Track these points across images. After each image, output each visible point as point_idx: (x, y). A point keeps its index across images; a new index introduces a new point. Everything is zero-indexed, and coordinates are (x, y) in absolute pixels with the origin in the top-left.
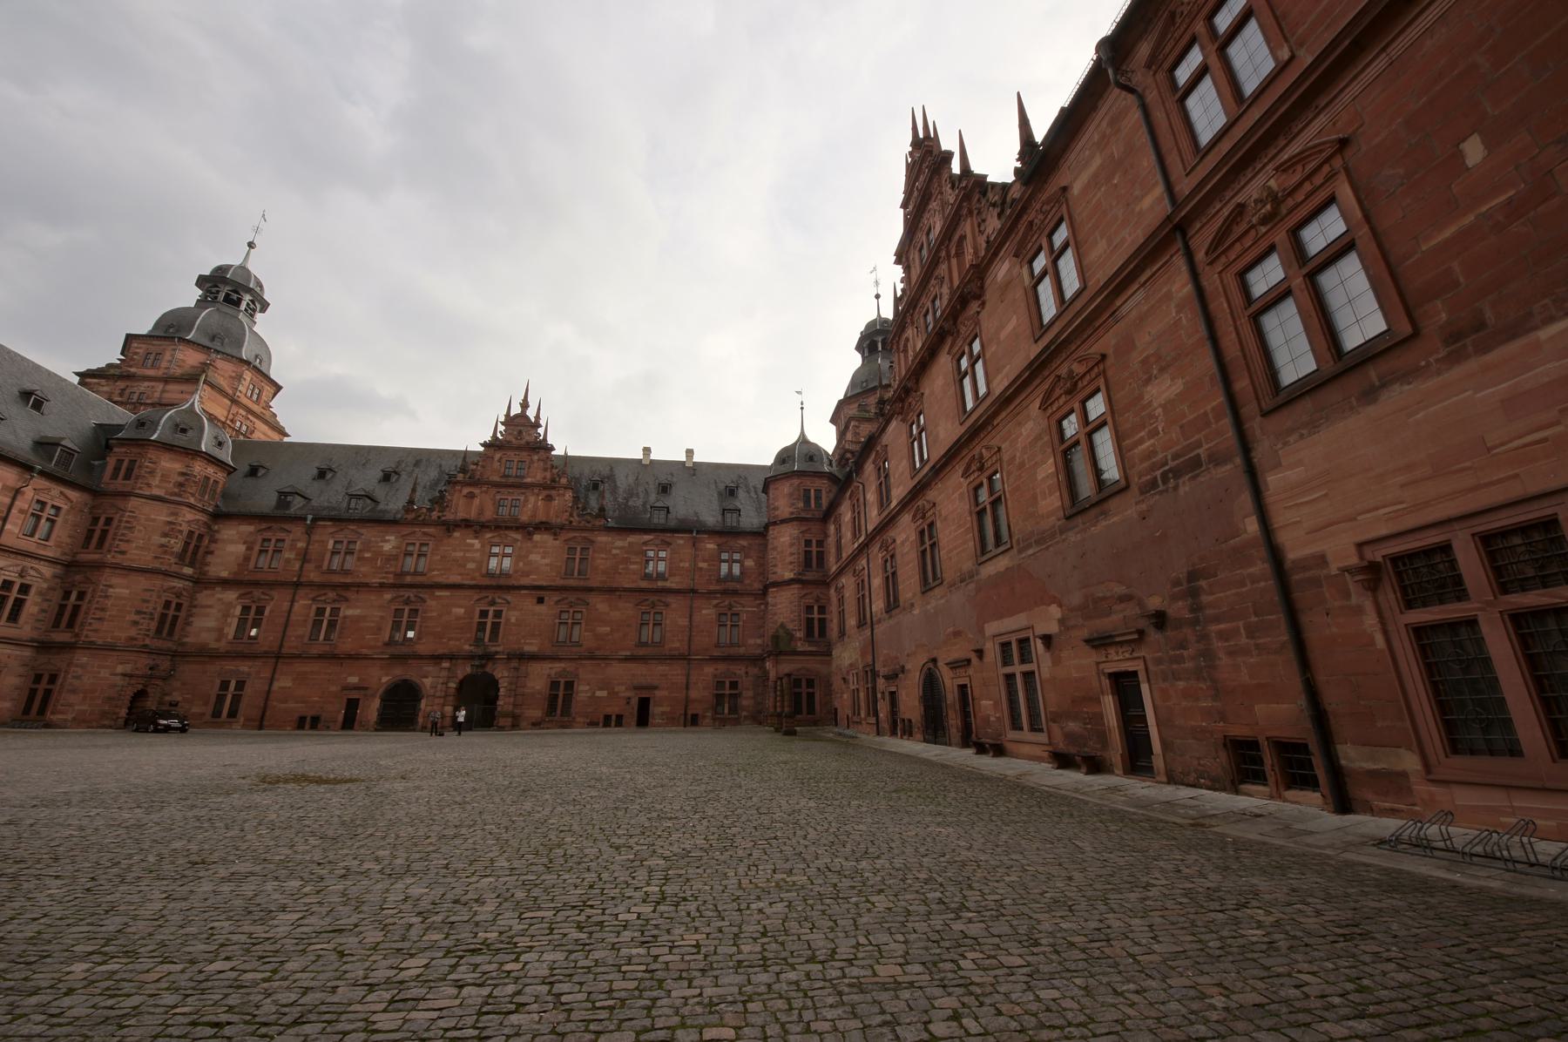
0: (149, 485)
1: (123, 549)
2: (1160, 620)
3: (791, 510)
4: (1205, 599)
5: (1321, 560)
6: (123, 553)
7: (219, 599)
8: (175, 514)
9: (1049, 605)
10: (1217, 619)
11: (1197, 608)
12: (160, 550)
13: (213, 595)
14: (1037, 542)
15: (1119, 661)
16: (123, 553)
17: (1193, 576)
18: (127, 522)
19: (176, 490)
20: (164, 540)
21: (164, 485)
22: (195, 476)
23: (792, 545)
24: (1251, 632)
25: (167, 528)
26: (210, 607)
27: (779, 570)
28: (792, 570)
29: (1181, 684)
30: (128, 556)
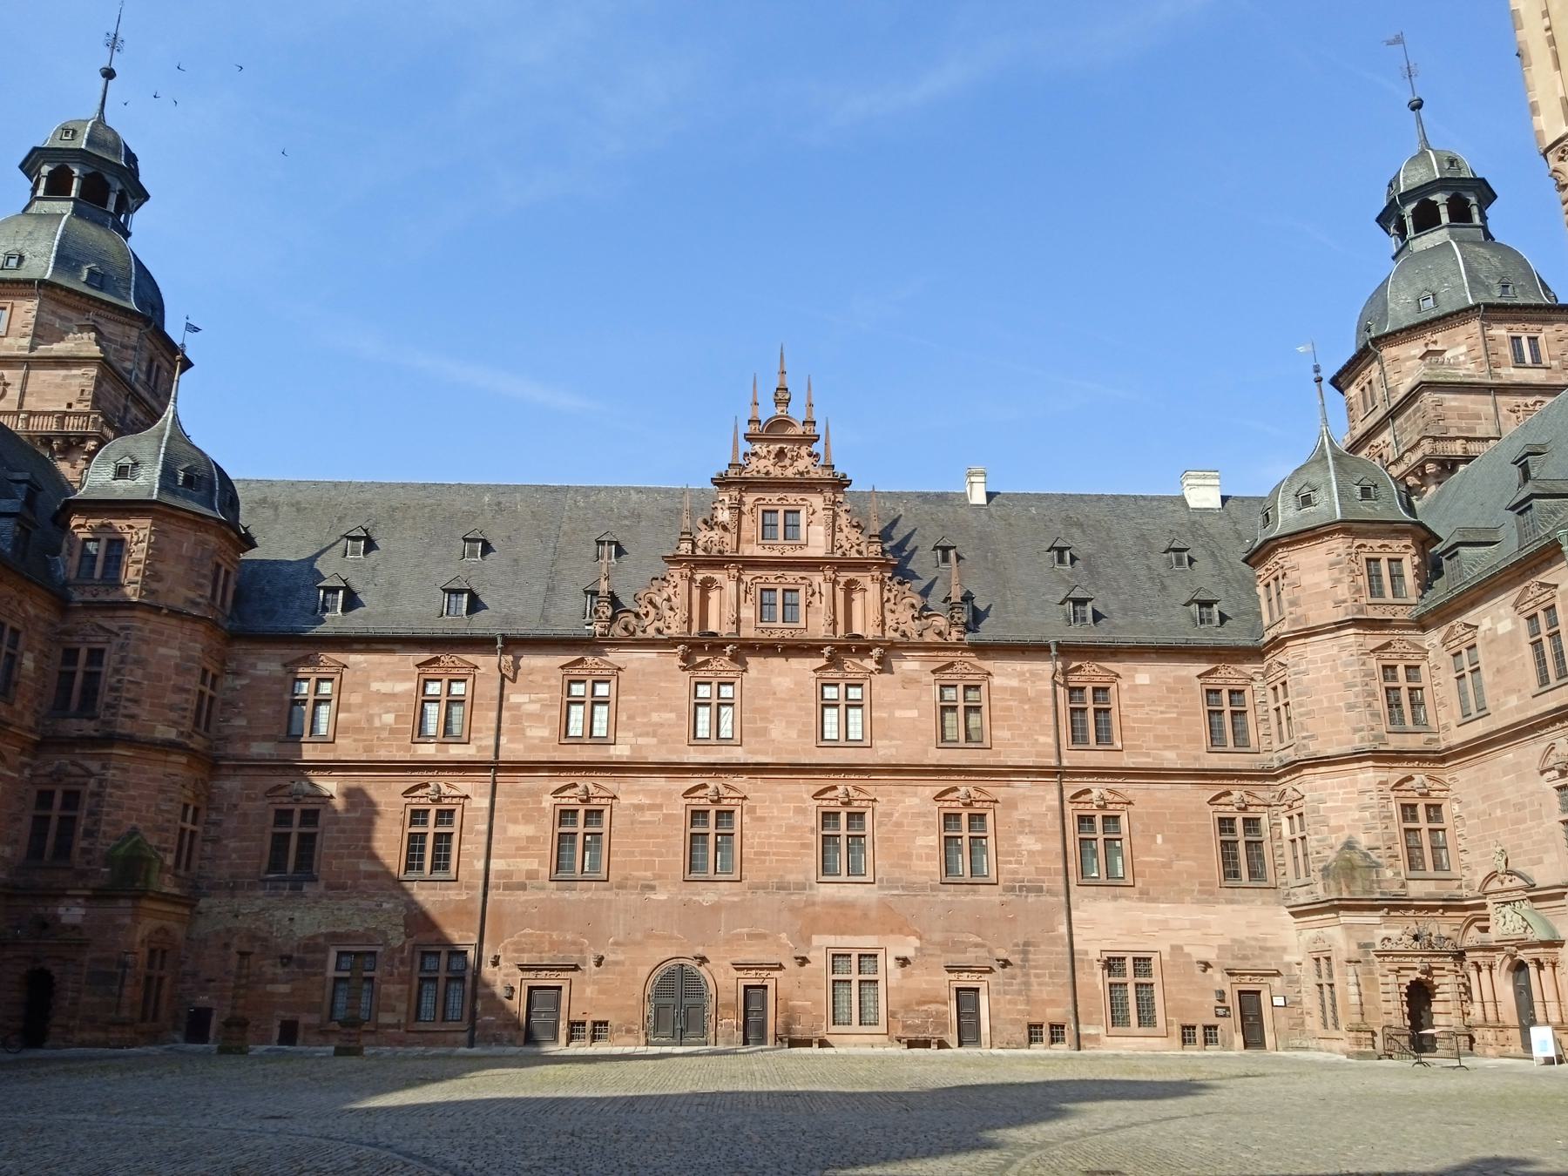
2: (1006, 963)
3: (191, 595)
4: (1031, 956)
5: (1086, 953)
9: (908, 936)
10: (1036, 967)
11: (1025, 960)
14: (903, 887)
15: (966, 980)
17: (1026, 944)
23: (180, 670)
24: (1051, 976)
27: (143, 712)
28: (174, 724)
29: (1008, 997)
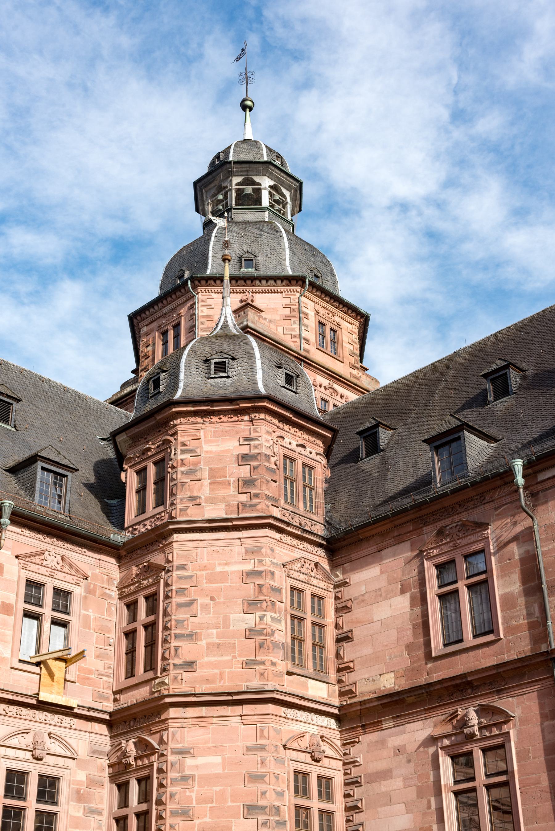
0: (195, 501)
1: (188, 658)
6: (189, 666)
7: (399, 750)
8: (251, 552)
12: (251, 643)
13: (382, 743)
16: (189, 666)
18: (180, 592)
19: (243, 498)
20: (251, 620)
21: (221, 492)
22: (267, 457)
25: (249, 590)
26: (386, 775)
30: (200, 672)
